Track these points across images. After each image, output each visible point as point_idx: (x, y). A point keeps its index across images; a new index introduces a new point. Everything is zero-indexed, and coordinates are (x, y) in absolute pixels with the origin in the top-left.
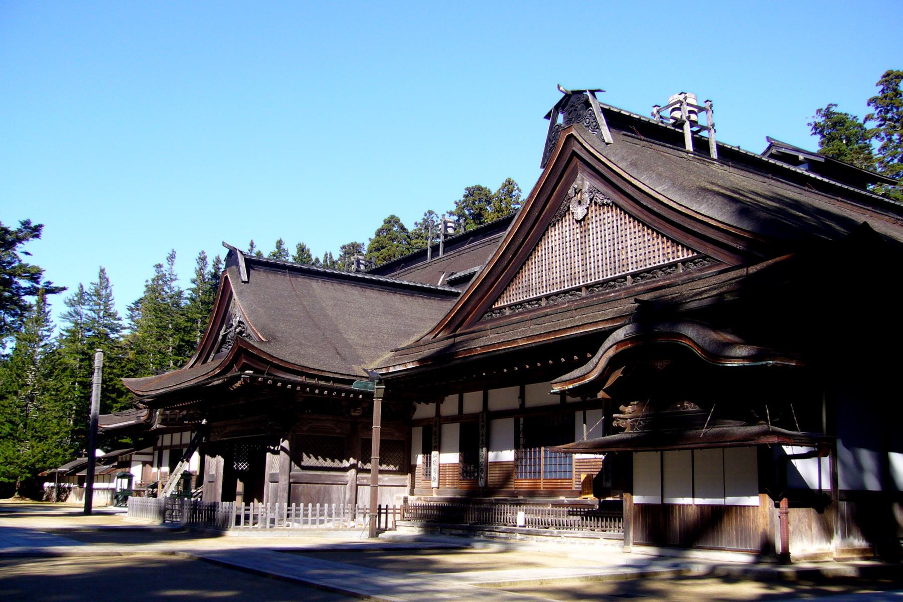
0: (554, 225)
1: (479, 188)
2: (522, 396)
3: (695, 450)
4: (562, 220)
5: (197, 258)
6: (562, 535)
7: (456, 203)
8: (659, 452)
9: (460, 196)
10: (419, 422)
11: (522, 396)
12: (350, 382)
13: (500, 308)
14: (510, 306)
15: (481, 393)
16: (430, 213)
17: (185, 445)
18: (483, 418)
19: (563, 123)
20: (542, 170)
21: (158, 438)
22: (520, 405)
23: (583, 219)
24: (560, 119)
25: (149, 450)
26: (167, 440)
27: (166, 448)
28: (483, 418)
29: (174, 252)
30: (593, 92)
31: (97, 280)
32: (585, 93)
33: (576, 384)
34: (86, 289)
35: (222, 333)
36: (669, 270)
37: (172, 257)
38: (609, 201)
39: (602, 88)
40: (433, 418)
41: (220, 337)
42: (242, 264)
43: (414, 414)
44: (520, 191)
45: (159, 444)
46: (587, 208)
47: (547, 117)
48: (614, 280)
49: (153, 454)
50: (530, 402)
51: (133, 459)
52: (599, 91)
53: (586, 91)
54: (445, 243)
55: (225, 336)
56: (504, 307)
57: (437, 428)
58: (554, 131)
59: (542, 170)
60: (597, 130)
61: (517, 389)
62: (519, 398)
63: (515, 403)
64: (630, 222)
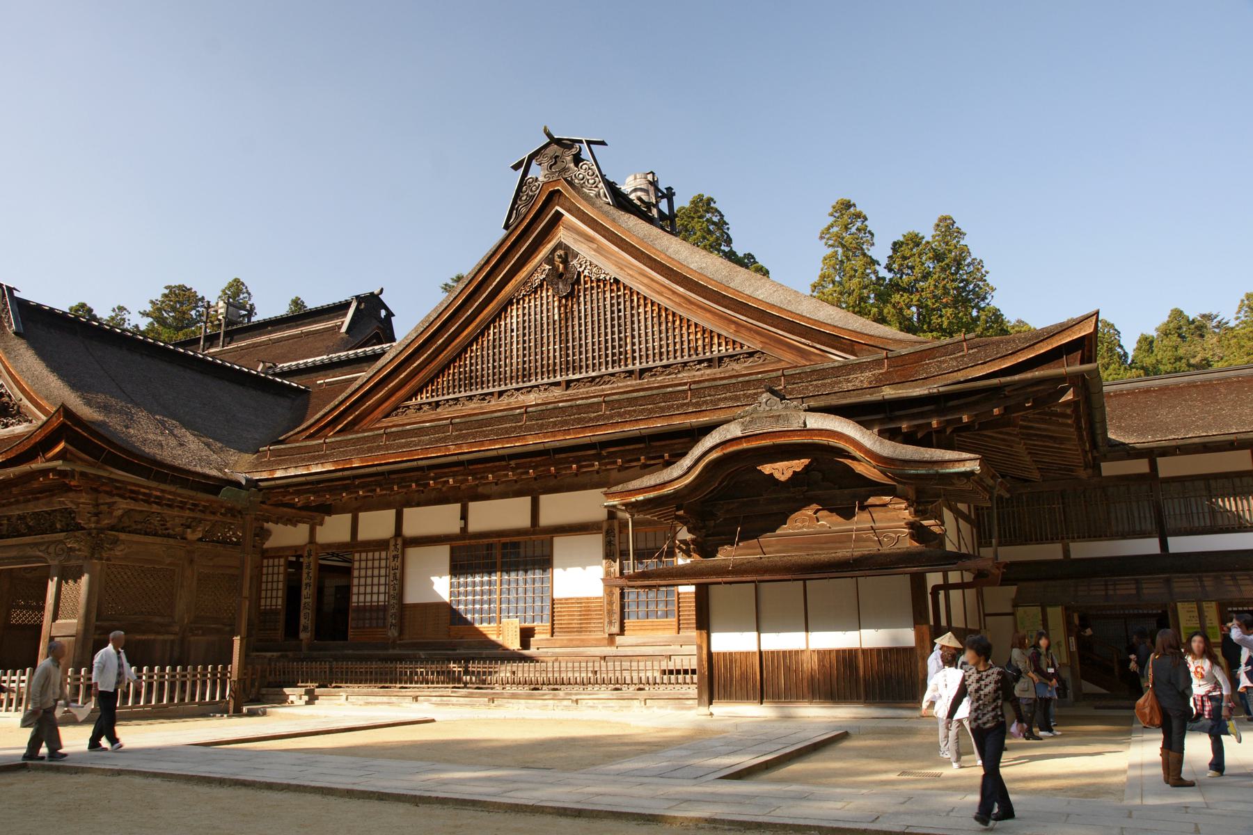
0: (518, 303)
1: (183, 288)
2: (464, 516)
3: (807, 582)
8: (855, 579)
10: (278, 552)
11: (464, 516)
15: (393, 512)
16: (121, 309)
18: (396, 545)
20: (505, 232)
23: (566, 297)
24: (538, 172)
28: (396, 545)
30: (589, 143)
33: (651, 495)
36: (698, 366)
40: (306, 545)
43: (267, 540)
44: (249, 294)
46: (573, 285)
47: (516, 167)
48: (613, 375)
50: (475, 526)
52: (603, 143)
53: (581, 142)
54: (227, 334)
57: (311, 558)
59: (505, 232)
60: (596, 189)
61: (457, 507)
62: (461, 519)
63: (454, 527)
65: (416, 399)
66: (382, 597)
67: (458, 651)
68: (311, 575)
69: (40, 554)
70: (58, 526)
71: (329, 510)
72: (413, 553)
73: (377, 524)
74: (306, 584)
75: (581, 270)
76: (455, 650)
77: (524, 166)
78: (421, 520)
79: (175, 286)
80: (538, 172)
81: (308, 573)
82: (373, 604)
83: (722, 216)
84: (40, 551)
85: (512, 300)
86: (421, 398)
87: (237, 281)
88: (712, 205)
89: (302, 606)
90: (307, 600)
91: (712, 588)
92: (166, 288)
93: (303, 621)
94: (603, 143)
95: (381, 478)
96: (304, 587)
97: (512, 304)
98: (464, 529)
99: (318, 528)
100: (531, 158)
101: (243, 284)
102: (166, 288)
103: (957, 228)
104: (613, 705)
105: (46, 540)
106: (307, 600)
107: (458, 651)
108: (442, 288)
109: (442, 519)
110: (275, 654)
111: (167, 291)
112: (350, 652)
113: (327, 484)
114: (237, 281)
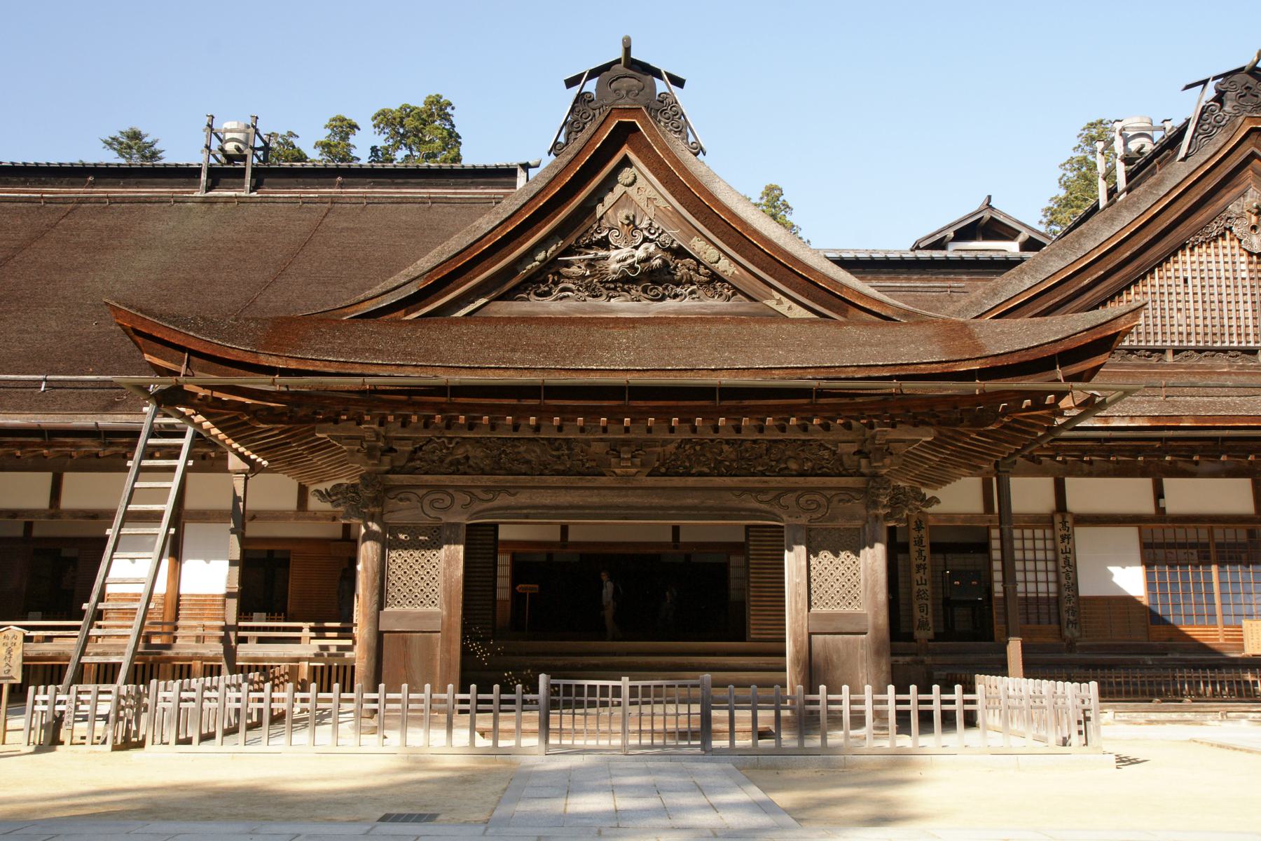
0: (1192, 249)
2: (1159, 494)
11: (1159, 494)
66: (1042, 587)
67: (1170, 656)
68: (924, 554)
69: (763, 506)
74: (919, 566)
76: (1166, 654)
81: (920, 552)
82: (1051, 595)
83: (453, 126)
84: (761, 502)
88: (449, 110)
89: (915, 594)
90: (922, 587)
93: (918, 614)
95: (1210, 443)
96: (914, 570)
103: (784, 201)
105: (773, 485)
106: (922, 587)
107: (1170, 656)
108: (106, 142)
113: (1120, 443)
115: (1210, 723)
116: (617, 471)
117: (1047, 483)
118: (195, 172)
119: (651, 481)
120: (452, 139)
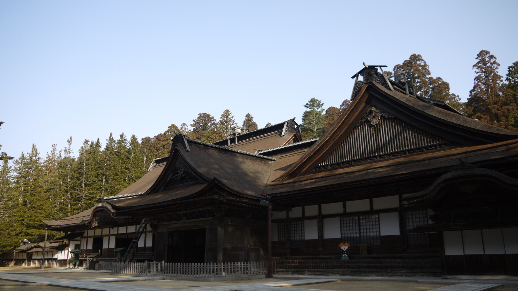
2: (344, 206)
4: (363, 125)
5: (84, 142)
6: (394, 272)
7: (193, 120)
9: (196, 117)
11: (344, 206)
12: (260, 201)
13: (324, 166)
14: (331, 165)
16: (184, 124)
17: (106, 236)
19: (363, 80)
21: (84, 232)
22: (344, 211)
25: (79, 238)
26: (91, 233)
27: (91, 237)
29: (71, 138)
30: (380, 66)
31: (30, 152)
32: (376, 67)
33: (419, 200)
34: (25, 155)
35: (170, 177)
37: (69, 141)
38: (393, 117)
39: (387, 66)
41: (168, 179)
42: (186, 142)
45: (85, 235)
47: (353, 77)
49: (80, 240)
51: (70, 243)
52: (385, 66)
53: (377, 66)
55: (171, 179)
56: (327, 165)
58: (357, 84)
60: (385, 84)
63: (341, 211)
64: (405, 126)
65: (322, 164)
70: (207, 215)
71: (294, 206)
72: (326, 221)
73: (312, 210)
75: (381, 114)
77: (356, 76)
78: (329, 208)
79: (202, 114)
80: (361, 78)
85: (356, 127)
86: (324, 164)
87: (227, 111)
91: (444, 232)
92: (199, 115)
94: (385, 66)
97: (356, 129)
98: (345, 211)
99: (290, 213)
100: (359, 73)
101: (230, 112)
102: (199, 115)
104: (408, 275)
109: (336, 208)
110: (278, 257)
111: (199, 116)
112: (305, 256)
114: (227, 111)
115: (330, 275)
116: (184, 219)
117: (317, 206)
118: (227, 141)
119: (187, 221)
120: (255, 124)
